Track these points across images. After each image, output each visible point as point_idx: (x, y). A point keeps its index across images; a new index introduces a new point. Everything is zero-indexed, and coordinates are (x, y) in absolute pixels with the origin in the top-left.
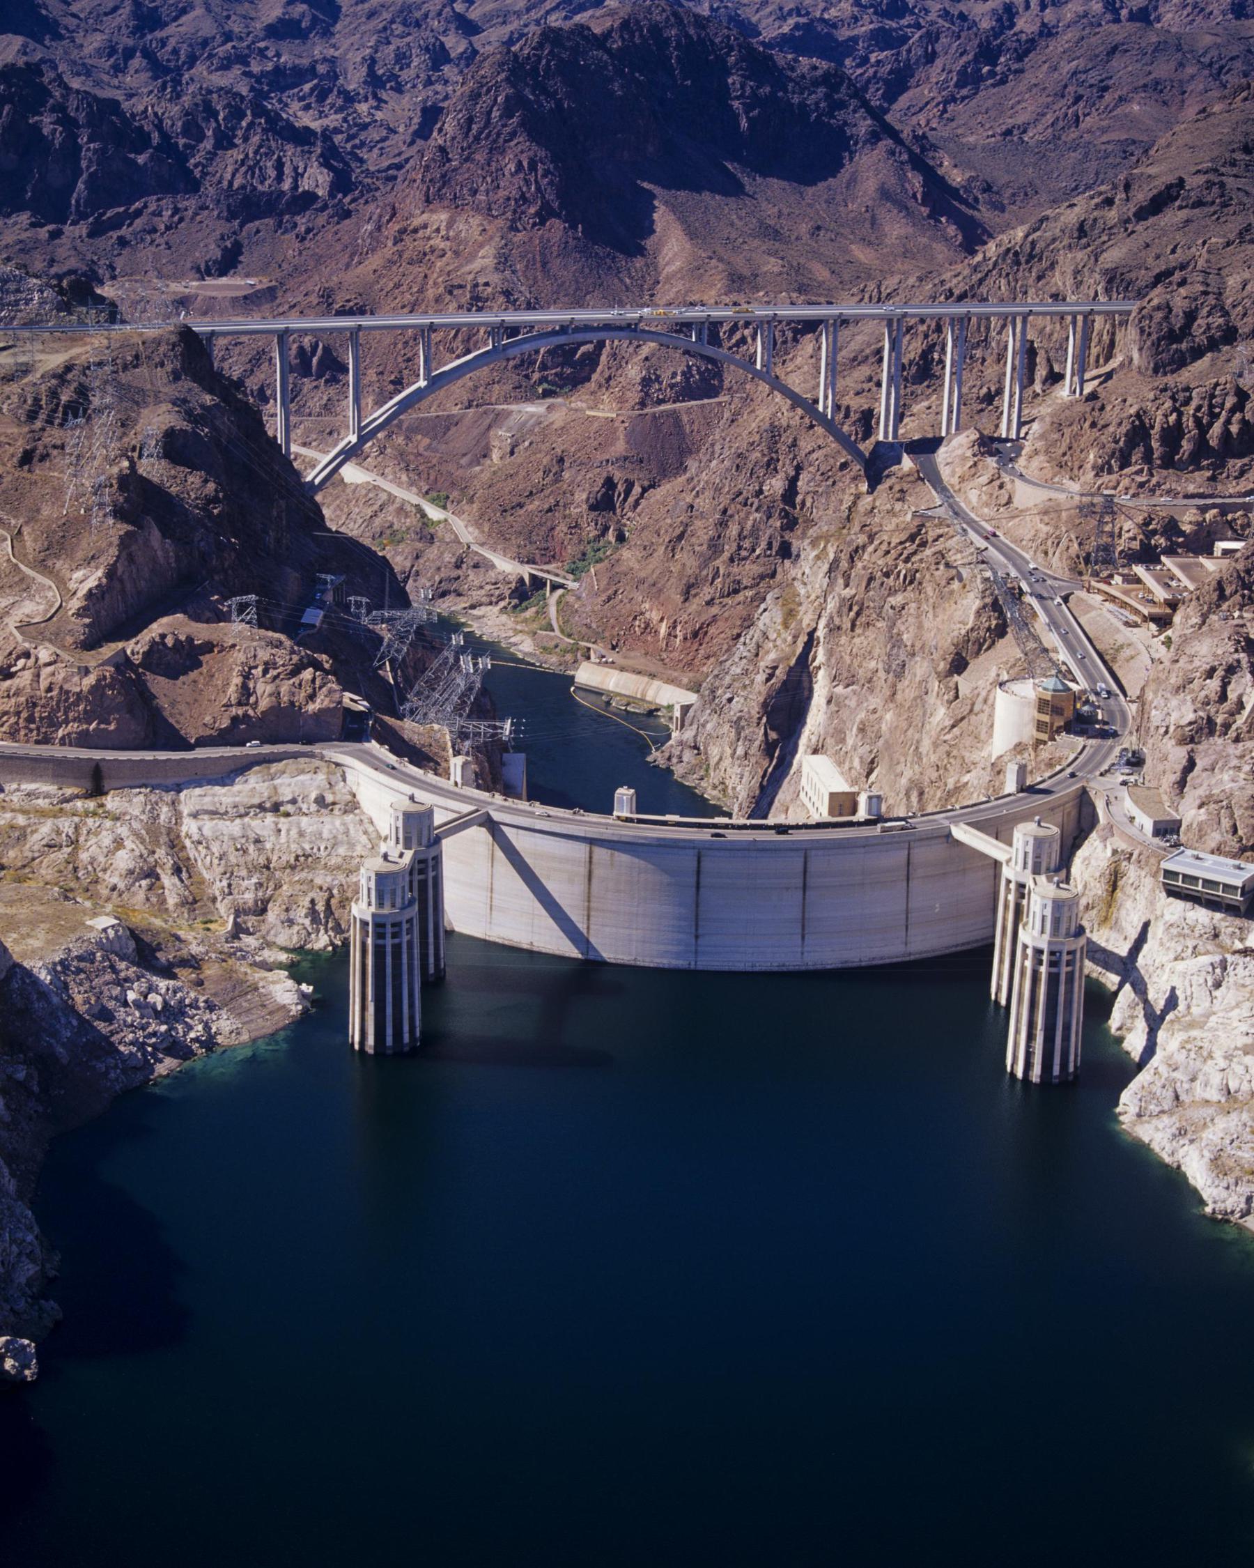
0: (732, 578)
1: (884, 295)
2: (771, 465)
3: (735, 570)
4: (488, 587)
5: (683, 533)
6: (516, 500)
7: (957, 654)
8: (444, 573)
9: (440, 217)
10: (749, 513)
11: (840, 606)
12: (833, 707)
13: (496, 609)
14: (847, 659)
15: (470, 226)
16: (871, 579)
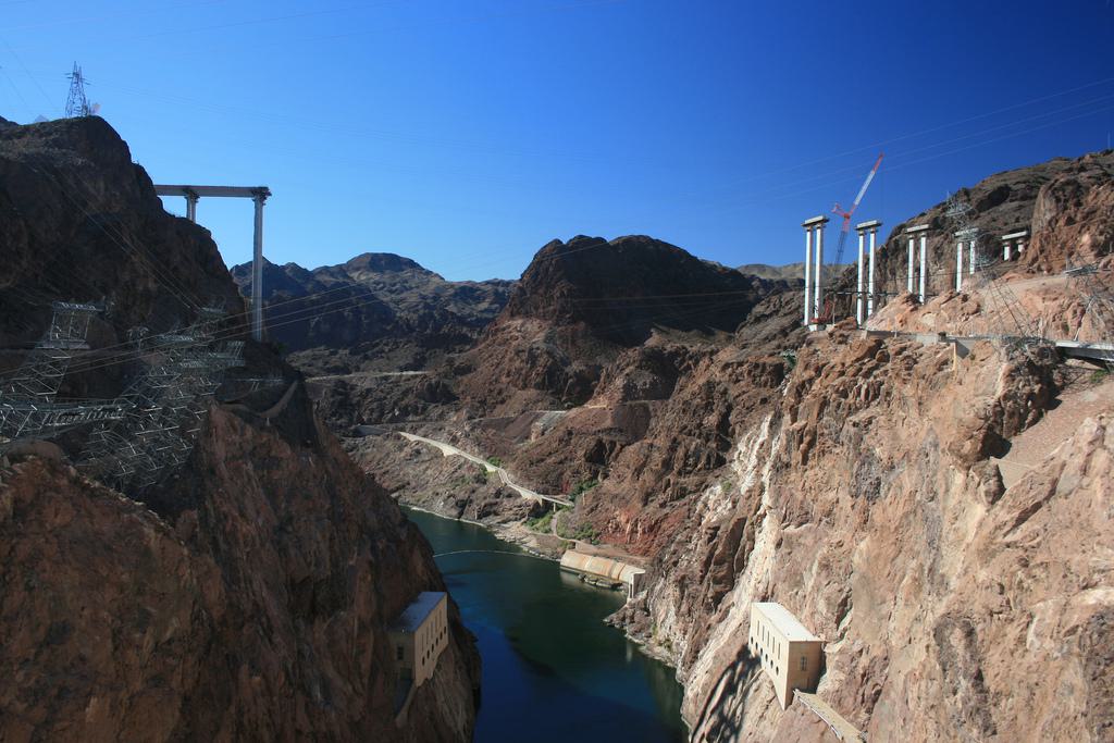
0: (679, 486)
1: (783, 304)
2: (708, 407)
3: (682, 480)
4: (515, 509)
5: (645, 462)
6: (539, 457)
7: (990, 428)
8: (487, 501)
9: (518, 322)
10: (692, 441)
11: (788, 442)
12: (784, 550)
13: (519, 523)
14: (799, 496)
15: (533, 326)
16: (824, 403)
